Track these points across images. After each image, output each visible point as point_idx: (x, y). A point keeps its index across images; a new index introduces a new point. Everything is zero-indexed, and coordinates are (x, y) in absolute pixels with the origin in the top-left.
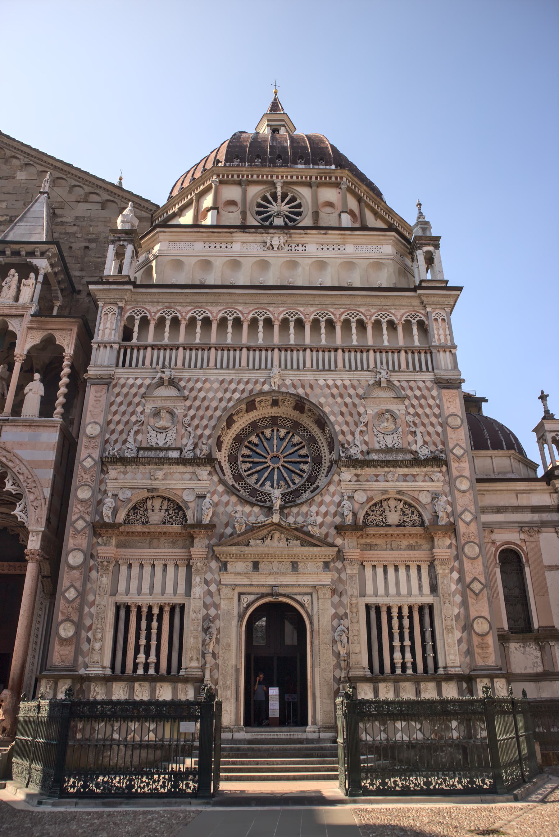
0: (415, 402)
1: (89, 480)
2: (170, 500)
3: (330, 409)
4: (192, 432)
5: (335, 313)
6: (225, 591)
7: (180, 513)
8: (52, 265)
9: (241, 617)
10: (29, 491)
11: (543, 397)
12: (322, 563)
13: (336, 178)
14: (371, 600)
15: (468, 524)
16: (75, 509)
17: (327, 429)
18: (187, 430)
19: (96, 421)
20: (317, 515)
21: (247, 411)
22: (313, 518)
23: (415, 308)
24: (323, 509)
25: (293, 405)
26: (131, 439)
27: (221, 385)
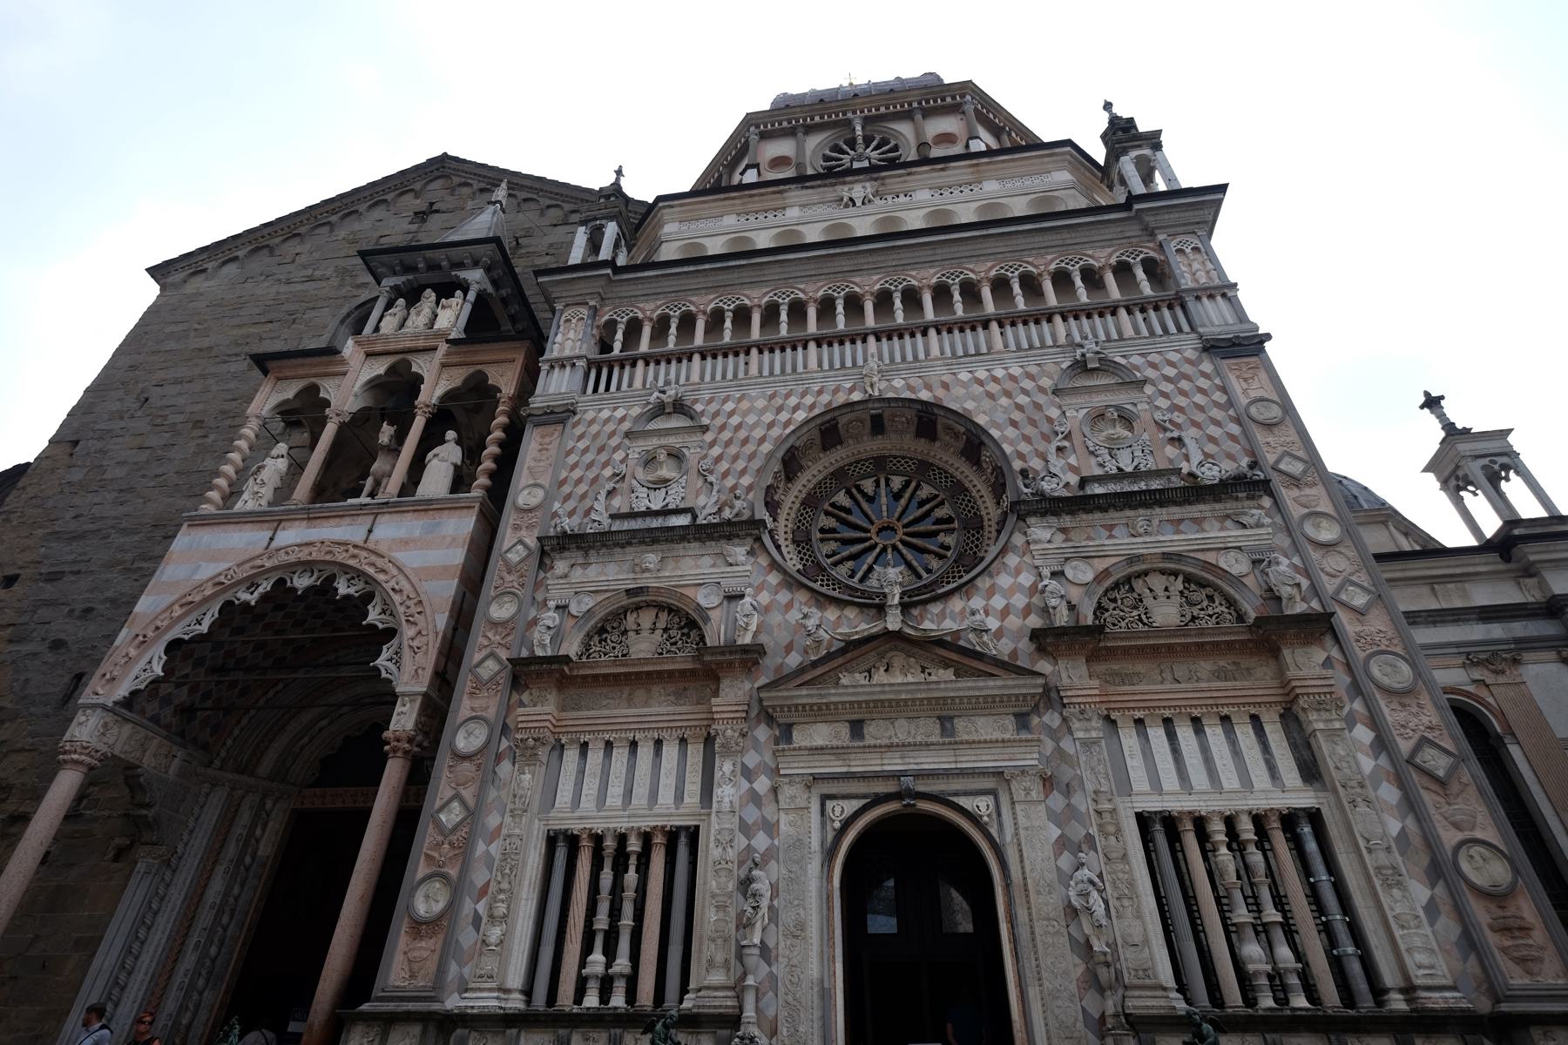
0: (1167, 387)
1: (515, 584)
2: (674, 610)
3: (987, 418)
5: (976, 269)
6: (787, 792)
8: (494, 282)
9: (829, 854)
10: (408, 621)
11: (1432, 403)
12: (1013, 718)
13: (954, 98)
14: (1153, 804)
15: (1360, 613)
16: (482, 641)
19: (539, 481)
20: (987, 613)
23: (1133, 240)
24: (998, 602)
25: (913, 428)
26: (600, 506)
27: (769, 402)
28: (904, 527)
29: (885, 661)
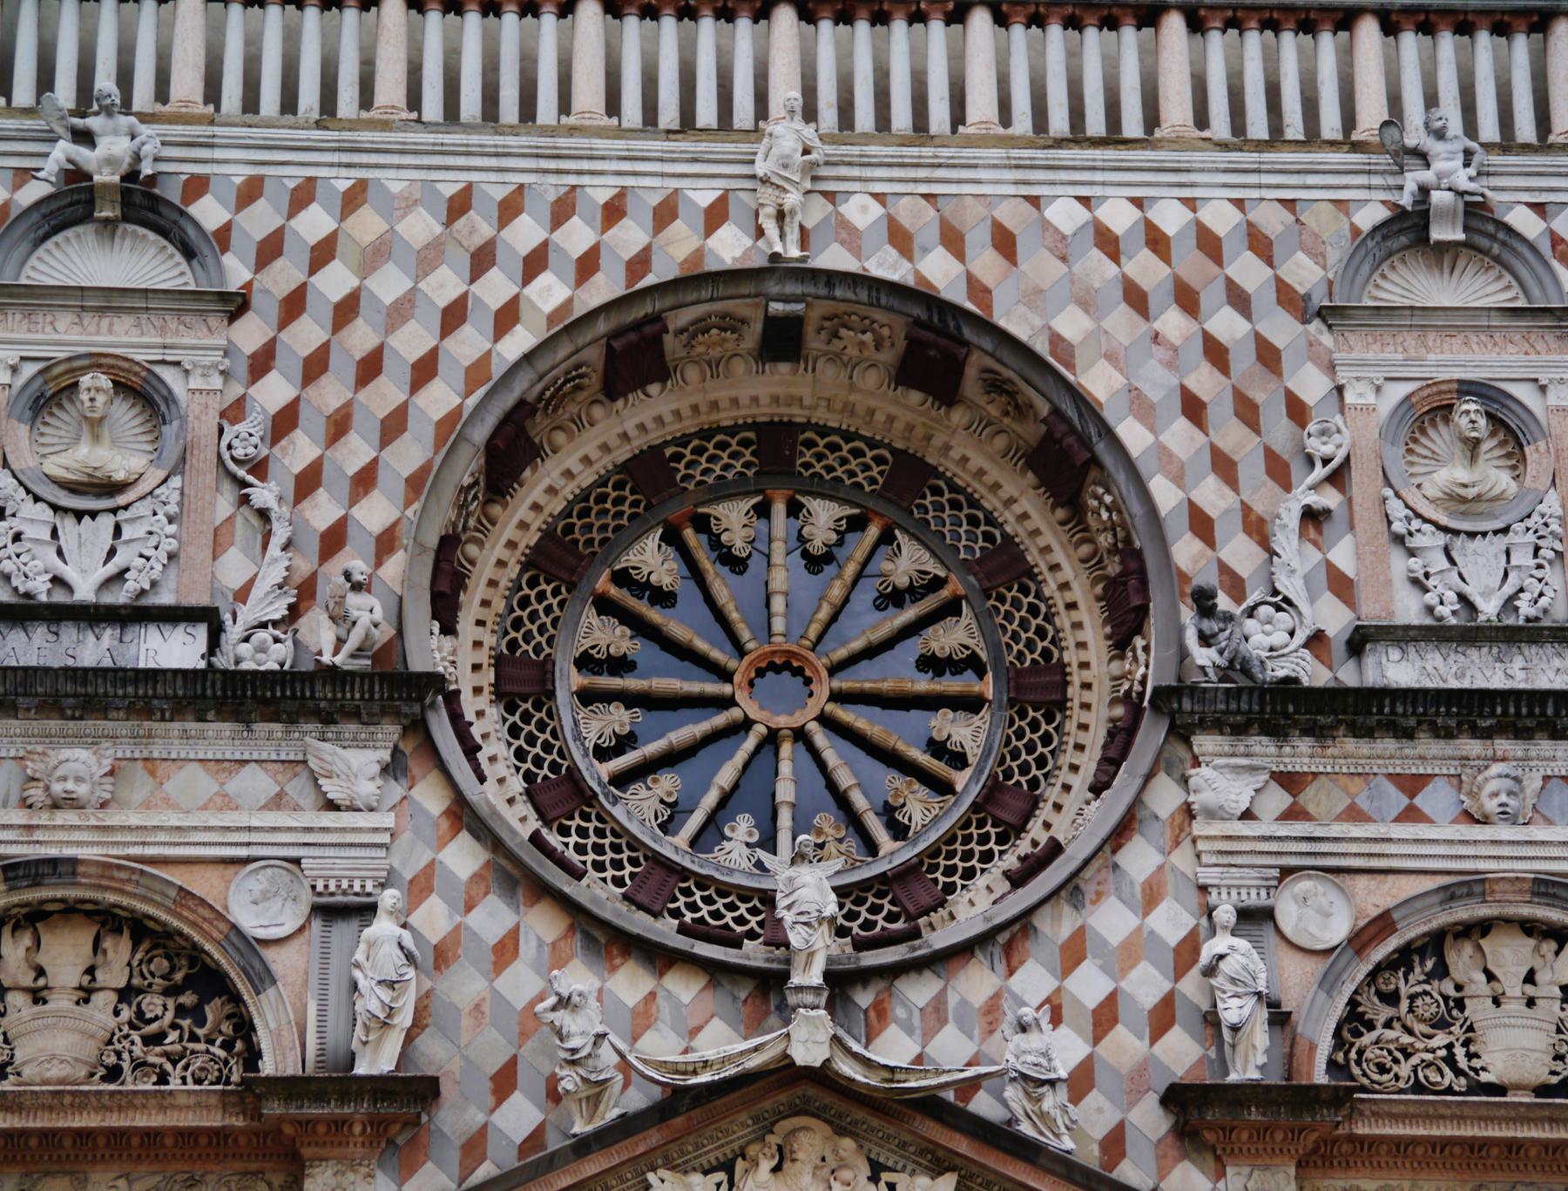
2: (150, 933)
3: (1119, 380)
4: (279, 511)
7: (211, 1011)
17: (1097, 500)
18: (245, 500)
20: (1056, 1020)
22: (1034, 1041)
24: (1089, 985)
25: (888, 356)
29: (773, 1140)
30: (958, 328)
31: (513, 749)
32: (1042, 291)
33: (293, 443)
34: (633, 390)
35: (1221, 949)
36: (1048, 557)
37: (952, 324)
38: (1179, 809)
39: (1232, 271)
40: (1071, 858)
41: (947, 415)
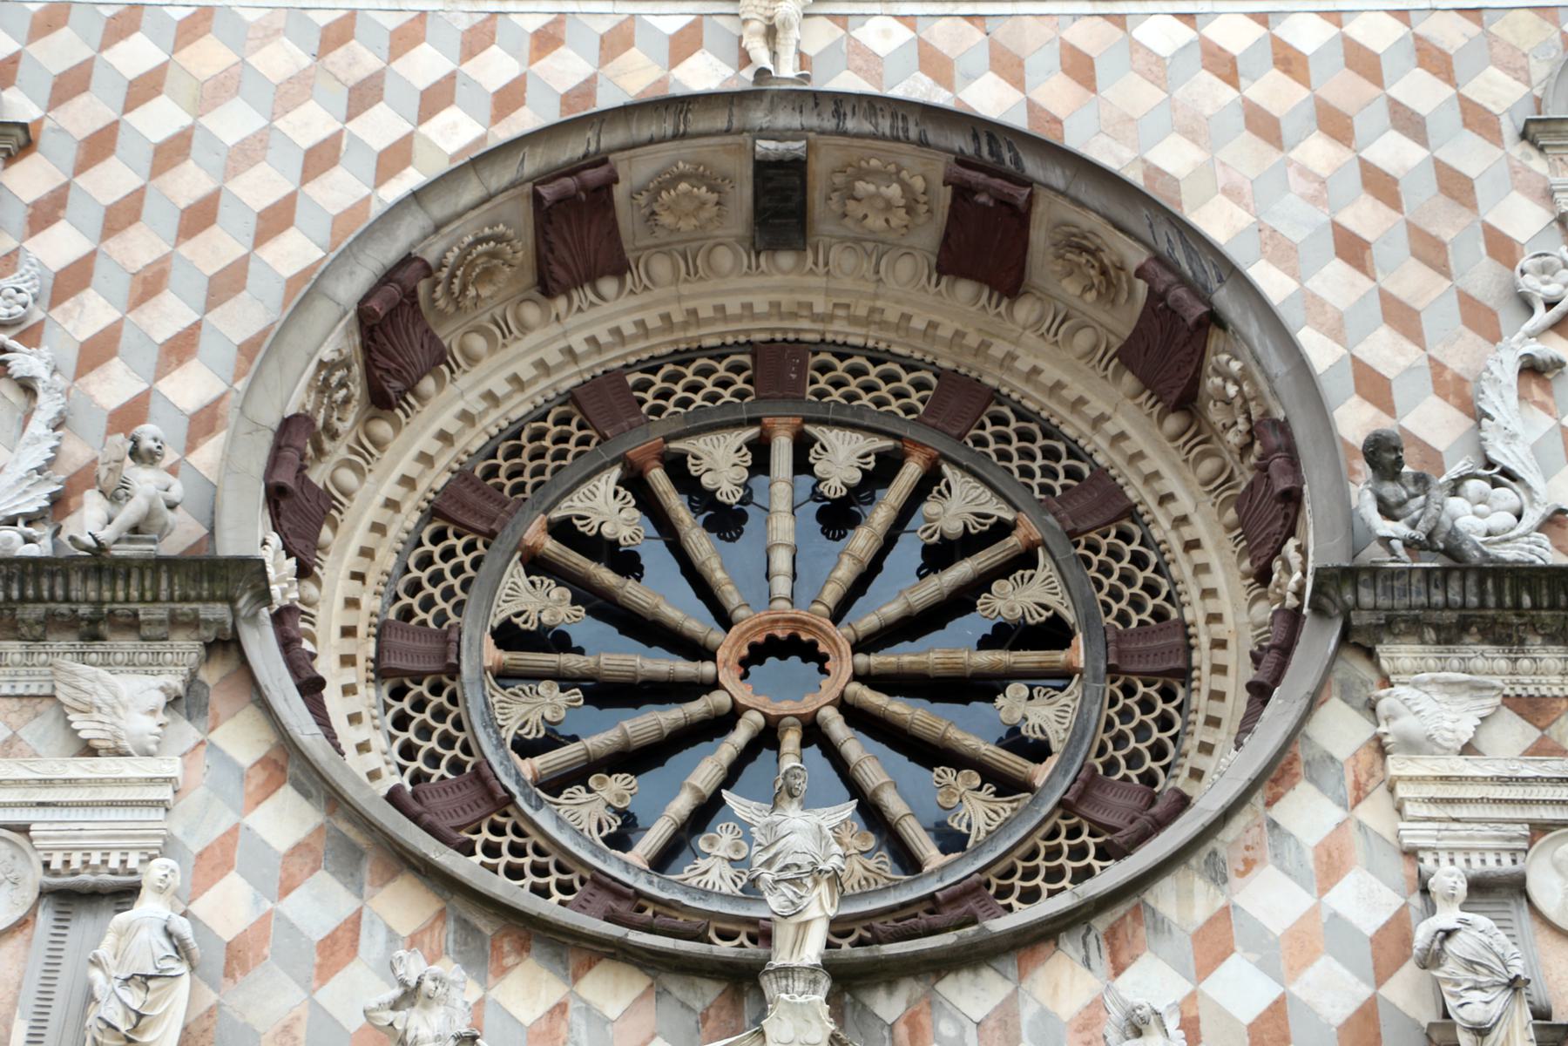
3: (1244, 218)
21: (548, 285)
25: (928, 237)
27: (318, 56)
28: (860, 646)
30: (1017, 161)
31: (397, 743)
32: (1132, 120)
33: (82, 305)
34: (578, 284)
35: (1450, 924)
36: (1157, 485)
37: (1007, 156)
38: (1367, 744)
39: (1396, 91)
40: (1205, 811)
41: (1010, 309)
